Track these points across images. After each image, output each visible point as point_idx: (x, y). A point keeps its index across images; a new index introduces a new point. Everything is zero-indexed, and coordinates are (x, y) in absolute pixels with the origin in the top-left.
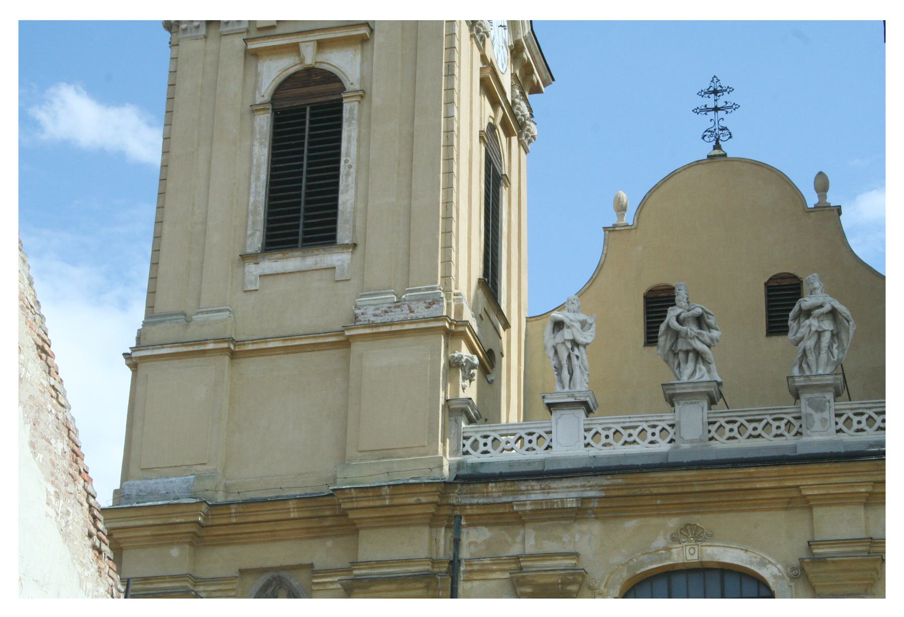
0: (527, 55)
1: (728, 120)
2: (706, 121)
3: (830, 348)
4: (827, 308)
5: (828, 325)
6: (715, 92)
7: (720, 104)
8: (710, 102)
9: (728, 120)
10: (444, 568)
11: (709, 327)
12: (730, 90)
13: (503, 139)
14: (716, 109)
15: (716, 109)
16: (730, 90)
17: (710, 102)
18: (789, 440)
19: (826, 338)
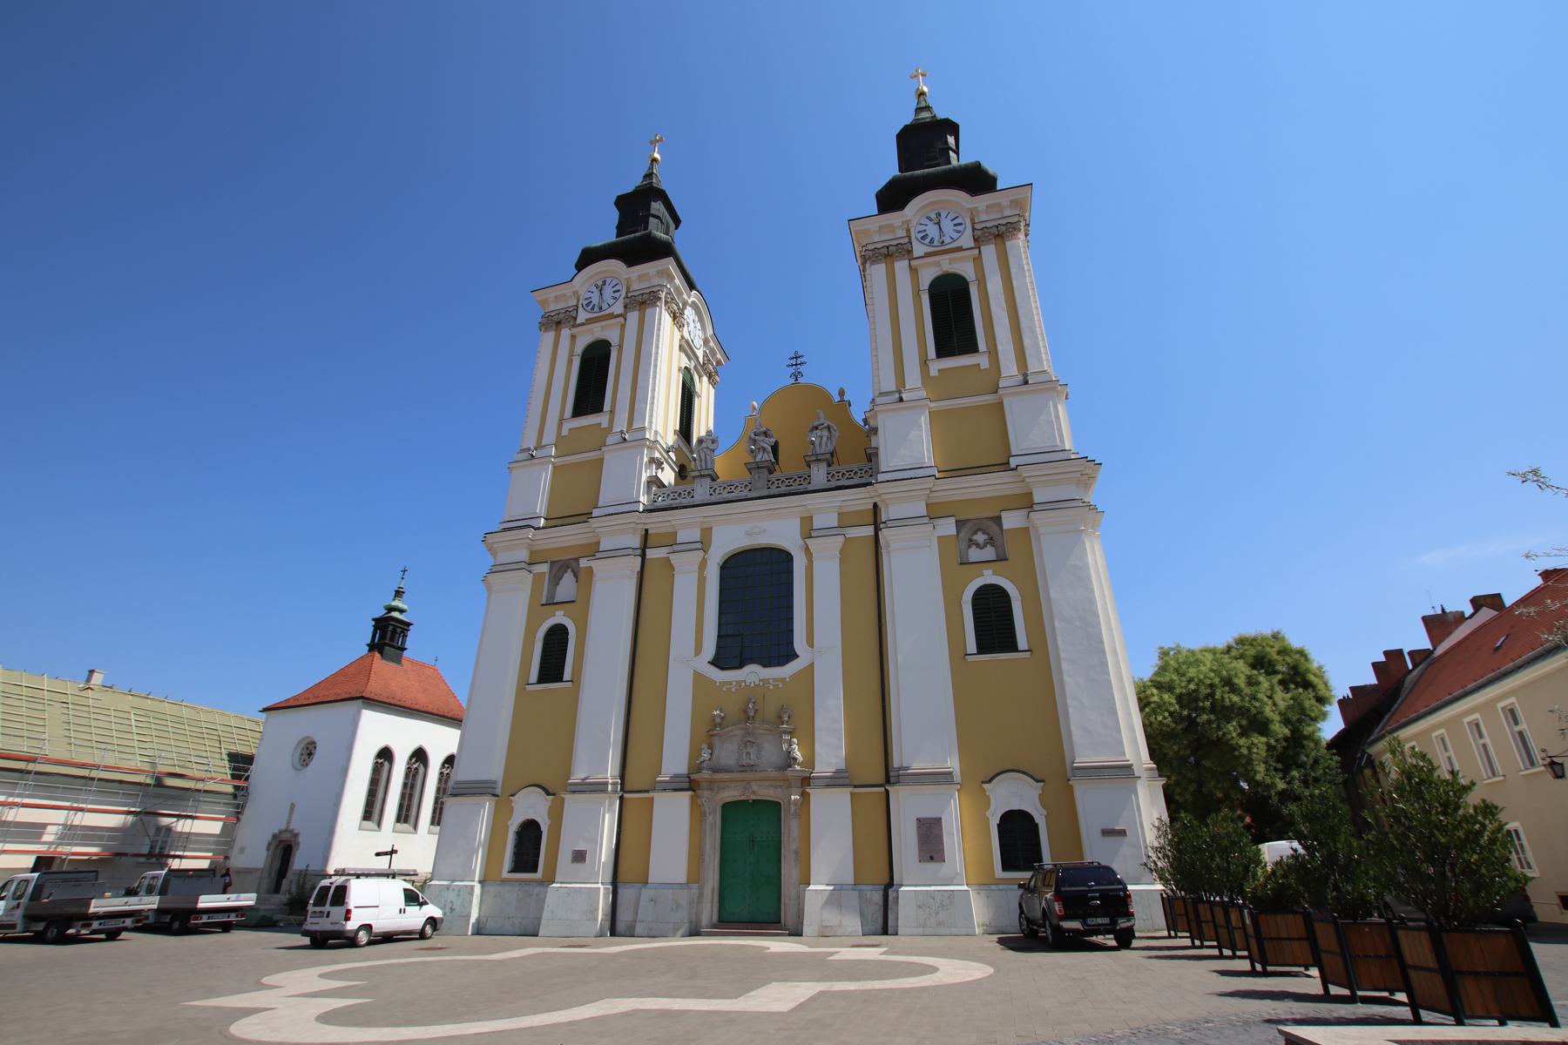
0: (712, 344)
1: (801, 369)
2: (792, 370)
3: (826, 444)
4: (826, 425)
5: (825, 433)
6: (796, 358)
7: (799, 362)
8: (794, 362)
9: (801, 369)
10: (639, 552)
11: (770, 437)
12: (802, 356)
13: (696, 377)
14: (796, 365)
15: (796, 365)
16: (802, 356)
17: (794, 362)
18: (805, 485)
19: (825, 439)
